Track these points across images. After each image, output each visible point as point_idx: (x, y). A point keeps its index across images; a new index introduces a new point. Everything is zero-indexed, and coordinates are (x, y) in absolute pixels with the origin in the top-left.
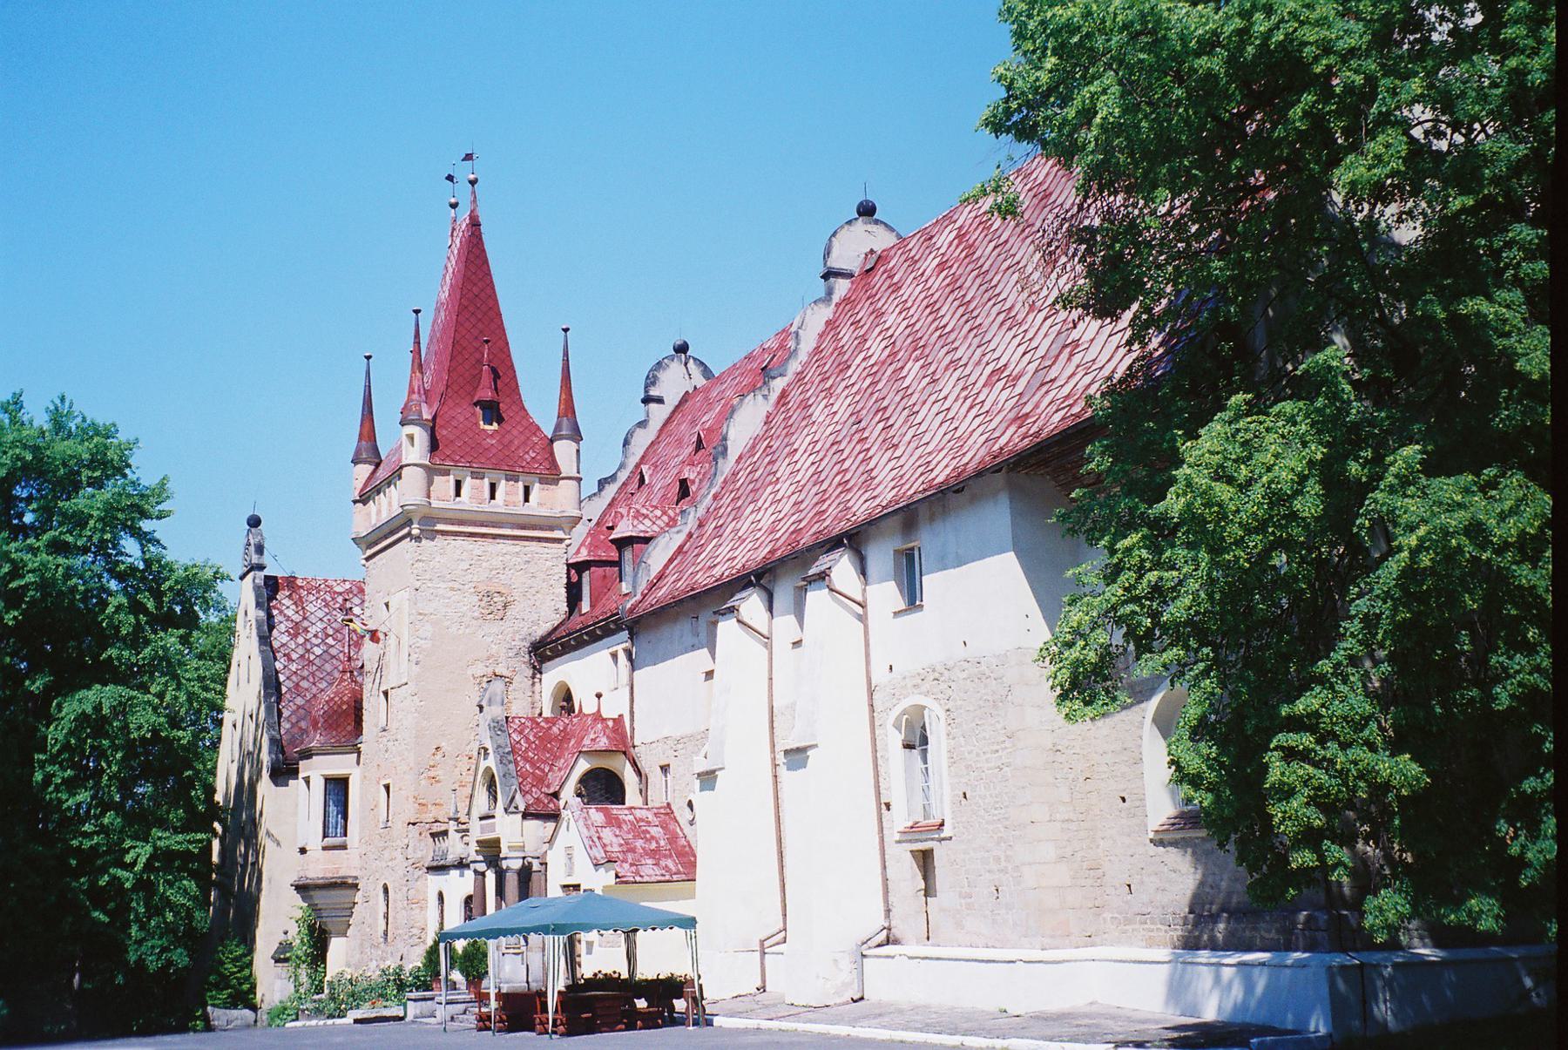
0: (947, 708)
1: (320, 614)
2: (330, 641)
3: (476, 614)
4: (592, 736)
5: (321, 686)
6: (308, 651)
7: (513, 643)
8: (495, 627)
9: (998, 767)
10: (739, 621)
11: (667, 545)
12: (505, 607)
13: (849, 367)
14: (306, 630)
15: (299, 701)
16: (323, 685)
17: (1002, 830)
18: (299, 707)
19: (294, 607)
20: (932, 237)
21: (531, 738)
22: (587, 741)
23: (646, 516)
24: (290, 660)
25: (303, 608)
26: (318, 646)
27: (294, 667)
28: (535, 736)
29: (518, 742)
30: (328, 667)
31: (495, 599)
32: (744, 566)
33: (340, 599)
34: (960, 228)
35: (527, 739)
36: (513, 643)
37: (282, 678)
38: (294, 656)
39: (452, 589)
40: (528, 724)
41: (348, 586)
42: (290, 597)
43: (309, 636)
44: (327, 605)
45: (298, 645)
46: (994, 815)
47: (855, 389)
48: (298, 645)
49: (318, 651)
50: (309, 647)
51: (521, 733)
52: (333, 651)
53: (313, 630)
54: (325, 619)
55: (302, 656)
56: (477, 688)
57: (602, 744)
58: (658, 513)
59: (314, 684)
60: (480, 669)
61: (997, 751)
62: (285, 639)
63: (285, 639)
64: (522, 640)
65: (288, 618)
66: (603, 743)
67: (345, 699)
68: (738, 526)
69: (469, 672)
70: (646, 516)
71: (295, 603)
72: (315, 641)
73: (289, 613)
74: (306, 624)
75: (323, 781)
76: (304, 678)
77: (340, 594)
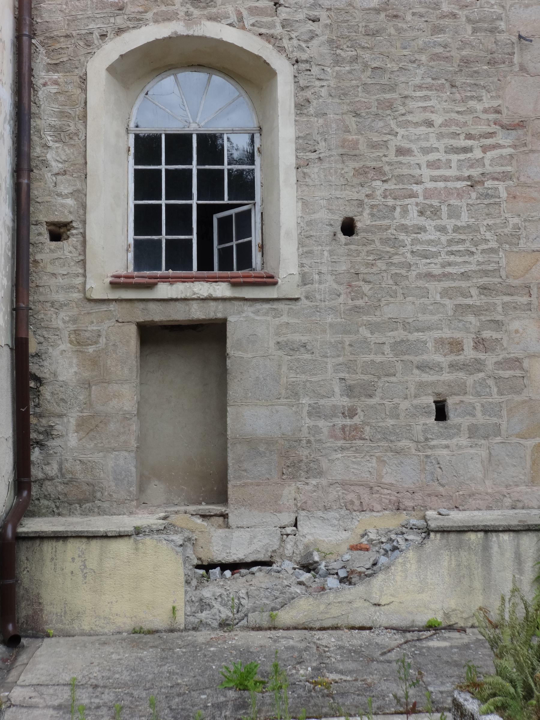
9: (469, 178)
61: (466, 150)
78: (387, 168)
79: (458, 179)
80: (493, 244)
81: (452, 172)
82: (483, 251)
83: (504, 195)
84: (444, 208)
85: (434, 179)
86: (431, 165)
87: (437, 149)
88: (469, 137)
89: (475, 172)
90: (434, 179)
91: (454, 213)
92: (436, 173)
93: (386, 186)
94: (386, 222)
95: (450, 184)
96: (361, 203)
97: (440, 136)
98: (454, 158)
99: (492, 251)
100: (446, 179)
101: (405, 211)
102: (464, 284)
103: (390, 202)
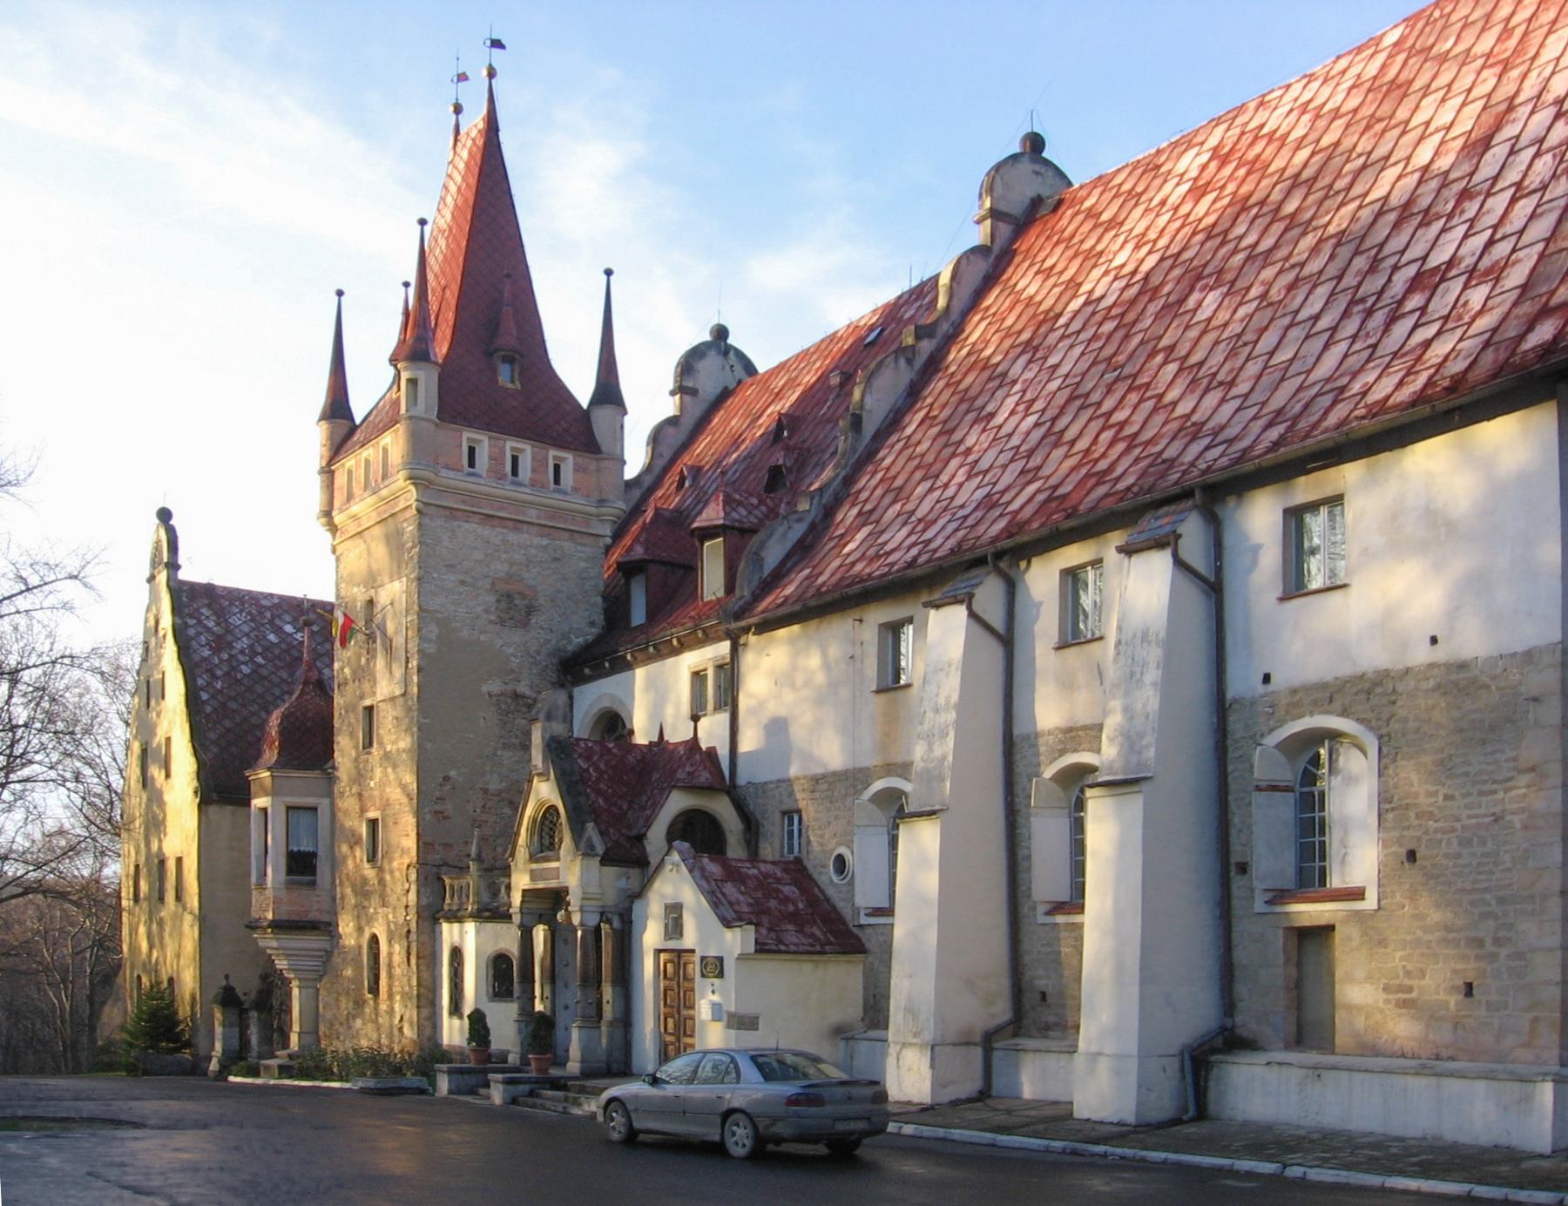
0: (1384, 731)
1: (246, 629)
2: (259, 660)
3: (493, 618)
4: (688, 769)
5: (252, 709)
6: (233, 668)
7: (538, 658)
8: (517, 637)
9: (1493, 814)
10: (972, 615)
11: (784, 535)
12: (529, 614)
13: (1059, 315)
14: (230, 645)
15: (227, 723)
16: (254, 708)
17: (1494, 902)
18: (228, 730)
19: (213, 618)
20: (1158, 167)
21: (602, 766)
22: (680, 775)
23: (740, 503)
24: (215, 677)
25: (226, 620)
26: (245, 663)
27: (219, 685)
28: (606, 765)
29: (587, 770)
30: (259, 689)
31: (516, 602)
32: (960, 544)
33: (268, 615)
34: (1215, 149)
35: (597, 768)
36: (538, 658)
37: (205, 696)
38: (219, 673)
39: (463, 582)
40: (597, 749)
41: (276, 601)
42: (209, 606)
43: (234, 652)
44: (253, 620)
45: (221, 661)
46: (1477, 881)
47: (1084, 336)
48: (221, 661)
49: (246, 669)
50: (235, 664)
51: (588, 758)
52: (264, 672)
53: (238, 646)
54: (252, 635)
55: (227, 674)
56: (493, 709)
57: (702, 779)
58: (755, 501)
59: (244, 706)
60: (495, 686)
62: (206, 653)
63: (206, 653)
64: (549, 655)
65: (208, 630)
66: (705, 777)
67: (310, 715)
68: (910, 507)
69: (485, 689)
70: (740, 503)
71: (215, 614)
72: (241, 657)
73: (211, 624)
74: (230, 638)
75: (283, 809)
76: (230, 698)
77: (268, 608)
78: (1436, 812)
79: (1485, 816)
80: (1509, 865)
81: (1482, 811)
82: (1502, 871)
83: (1518, 825)
84: (1475, 840)
85: (1470, 817)
86: (1468, 807)
87: (1471, 794)
88: (1495, 782)
89: (1497, 810)
90: (1470, 817)
91: (1483, 843)
92: (1471, 812)
93: (1437, 825)
94: (1436, 851)
95: (1480, 820)
96: (1419, 839)
97: (1474, 783)
98: (1484, 799)
99: (1509, 870)
100: (1477, 817)
101: (1449, 843)
102: (1488, 897)
103: (1439, 836)
